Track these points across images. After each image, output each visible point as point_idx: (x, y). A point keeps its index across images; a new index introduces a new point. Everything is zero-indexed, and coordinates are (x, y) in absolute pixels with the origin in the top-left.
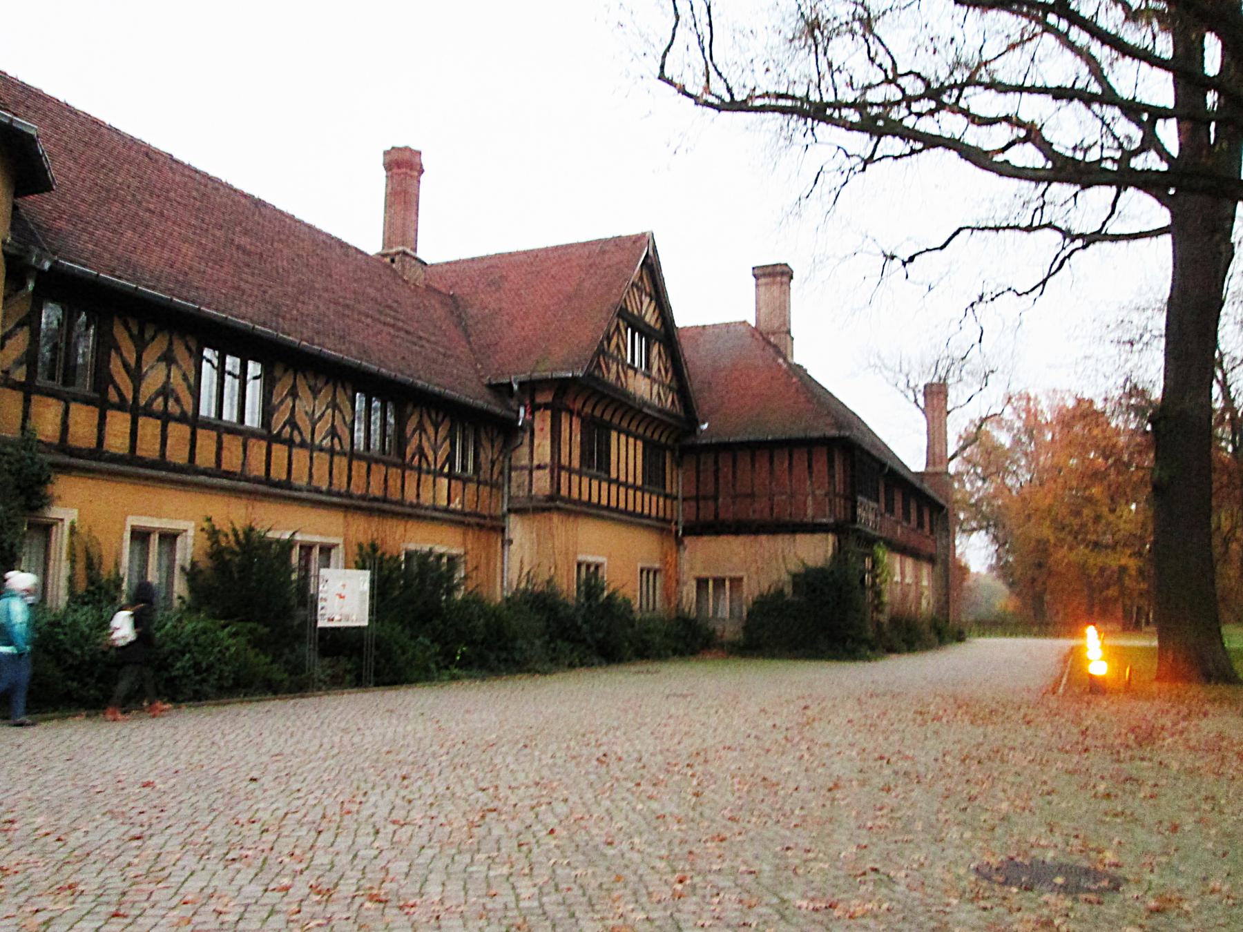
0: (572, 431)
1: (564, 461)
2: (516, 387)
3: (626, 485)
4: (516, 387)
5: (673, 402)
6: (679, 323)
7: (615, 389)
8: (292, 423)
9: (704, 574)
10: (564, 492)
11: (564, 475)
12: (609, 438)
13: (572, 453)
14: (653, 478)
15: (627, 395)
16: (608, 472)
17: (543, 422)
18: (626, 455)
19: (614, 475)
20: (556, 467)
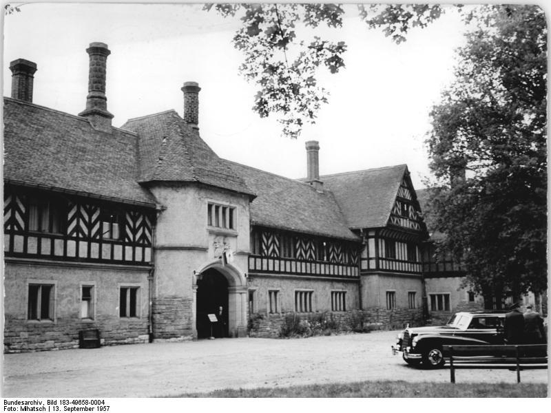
0: (382, 244)
1: (380, 256)
2: (362, 231)
3: (402, 261)
4: (362, 231)
5: (418, 228)
6: (415, 189)
7: (397, 227)
8: (301, 255)
9: (434, 293)
10: (381, 267)
11: (380, 261)
12: (395, 244)
13: (382, 253)
14: (411, 260)
15: (402, 228)
16: (395, 257)
17: (372, 242)
18: (401, 251)
19: (397, 258)
20: (378, 259)
